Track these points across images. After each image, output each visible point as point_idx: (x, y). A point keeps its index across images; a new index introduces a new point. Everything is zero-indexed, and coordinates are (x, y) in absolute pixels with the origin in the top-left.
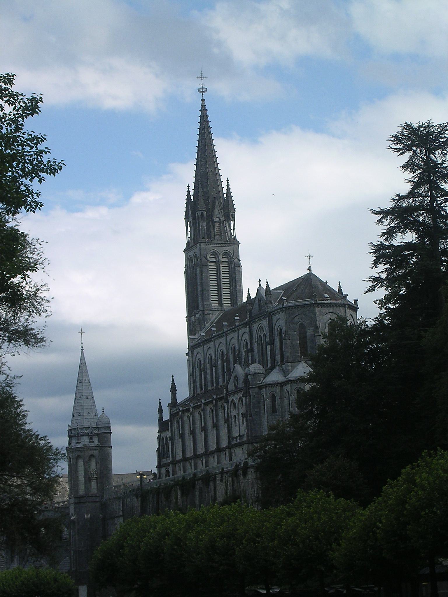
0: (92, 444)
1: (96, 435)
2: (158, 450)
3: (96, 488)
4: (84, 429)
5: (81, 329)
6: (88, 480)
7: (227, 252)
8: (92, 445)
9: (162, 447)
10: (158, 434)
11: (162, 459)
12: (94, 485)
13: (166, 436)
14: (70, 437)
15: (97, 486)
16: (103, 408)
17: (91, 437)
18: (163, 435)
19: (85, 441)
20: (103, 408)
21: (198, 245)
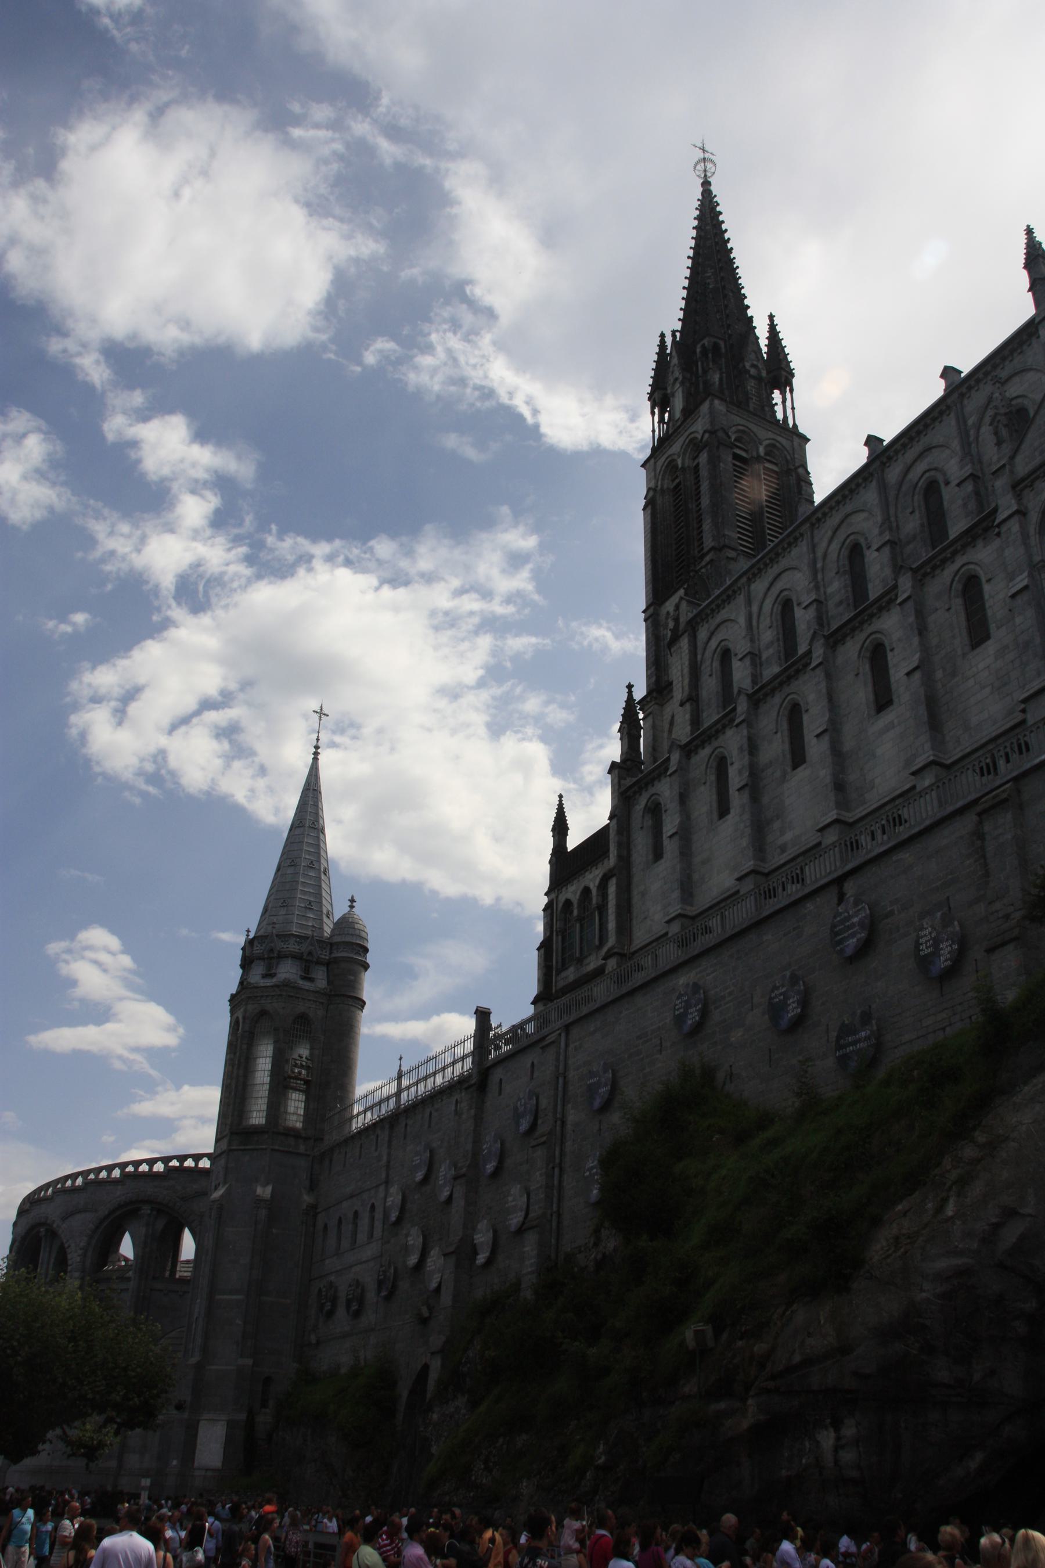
0: (309, 984)
1: (324, 965)
2: (545, 947)
3: (301, 1112)
4: (292, 940)
5: (321, 707)
6: (280, 1084)
7: (777, 444)
8: (306, 985)
9: (560, 937)
10: (545, 900)
11: (557, 975)
12: (296, 1105)
13: (587, 891)
14: (246, 963)
15: (306, 1109)
16: (353, 897)
17: (307, 963)
18: (572, 892)
19: (287, 971)
20: (353, 897)
21: (705, 407)
